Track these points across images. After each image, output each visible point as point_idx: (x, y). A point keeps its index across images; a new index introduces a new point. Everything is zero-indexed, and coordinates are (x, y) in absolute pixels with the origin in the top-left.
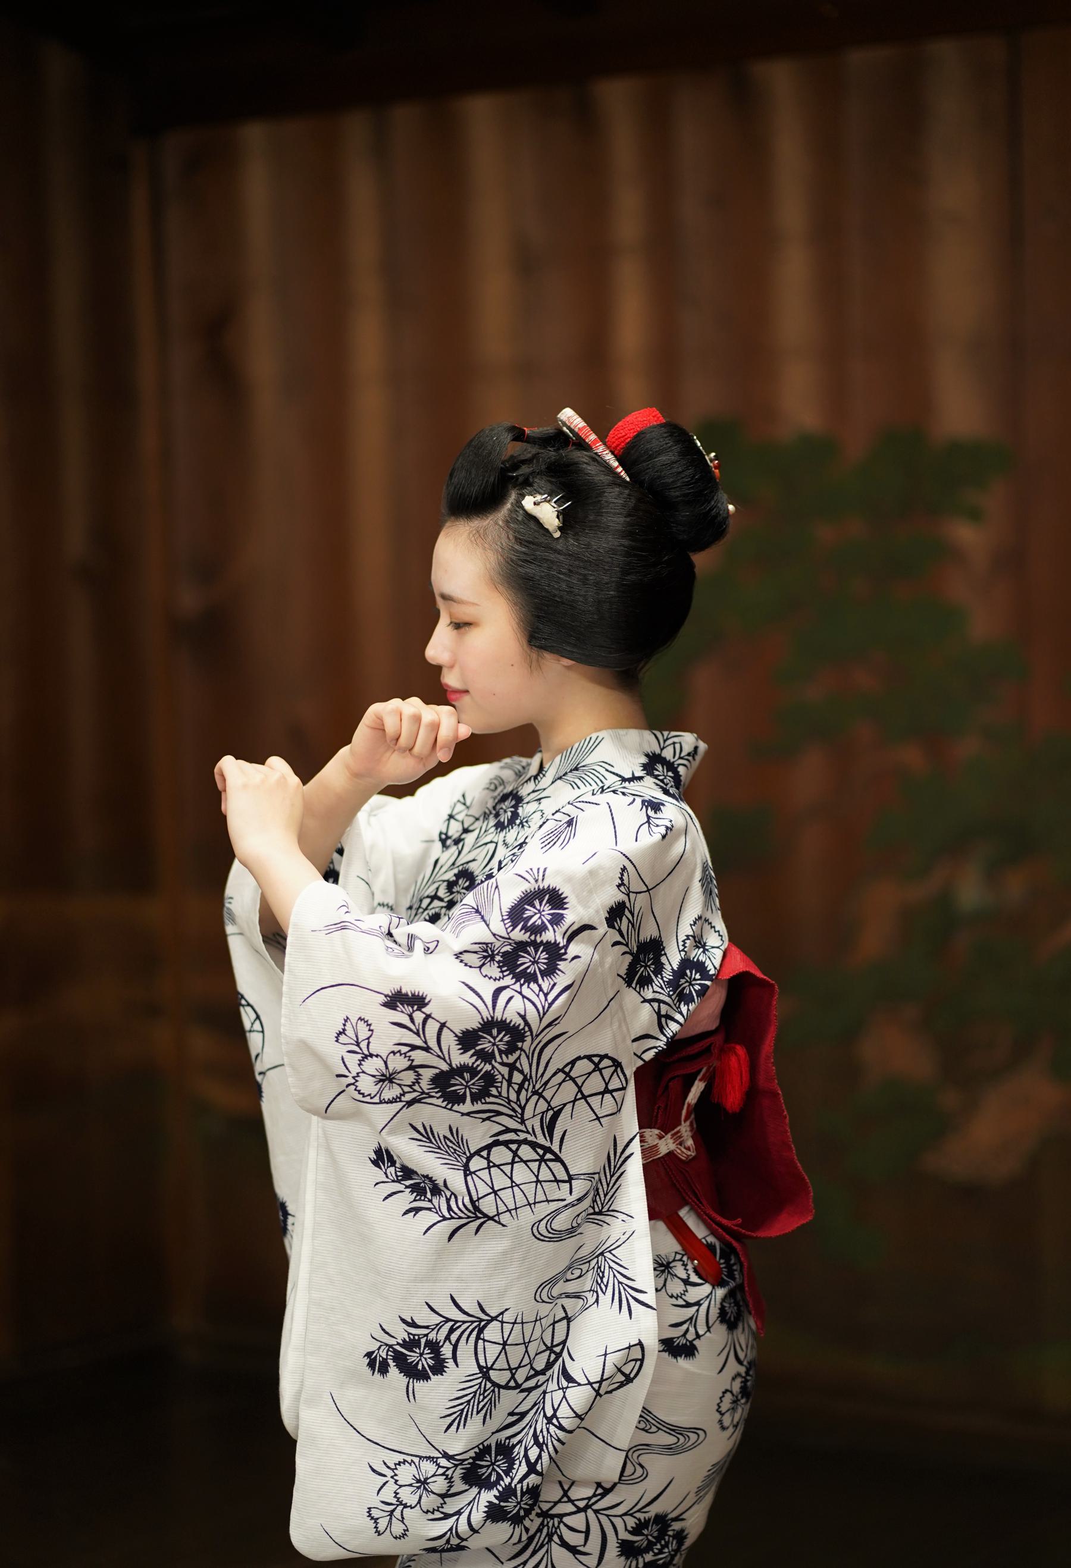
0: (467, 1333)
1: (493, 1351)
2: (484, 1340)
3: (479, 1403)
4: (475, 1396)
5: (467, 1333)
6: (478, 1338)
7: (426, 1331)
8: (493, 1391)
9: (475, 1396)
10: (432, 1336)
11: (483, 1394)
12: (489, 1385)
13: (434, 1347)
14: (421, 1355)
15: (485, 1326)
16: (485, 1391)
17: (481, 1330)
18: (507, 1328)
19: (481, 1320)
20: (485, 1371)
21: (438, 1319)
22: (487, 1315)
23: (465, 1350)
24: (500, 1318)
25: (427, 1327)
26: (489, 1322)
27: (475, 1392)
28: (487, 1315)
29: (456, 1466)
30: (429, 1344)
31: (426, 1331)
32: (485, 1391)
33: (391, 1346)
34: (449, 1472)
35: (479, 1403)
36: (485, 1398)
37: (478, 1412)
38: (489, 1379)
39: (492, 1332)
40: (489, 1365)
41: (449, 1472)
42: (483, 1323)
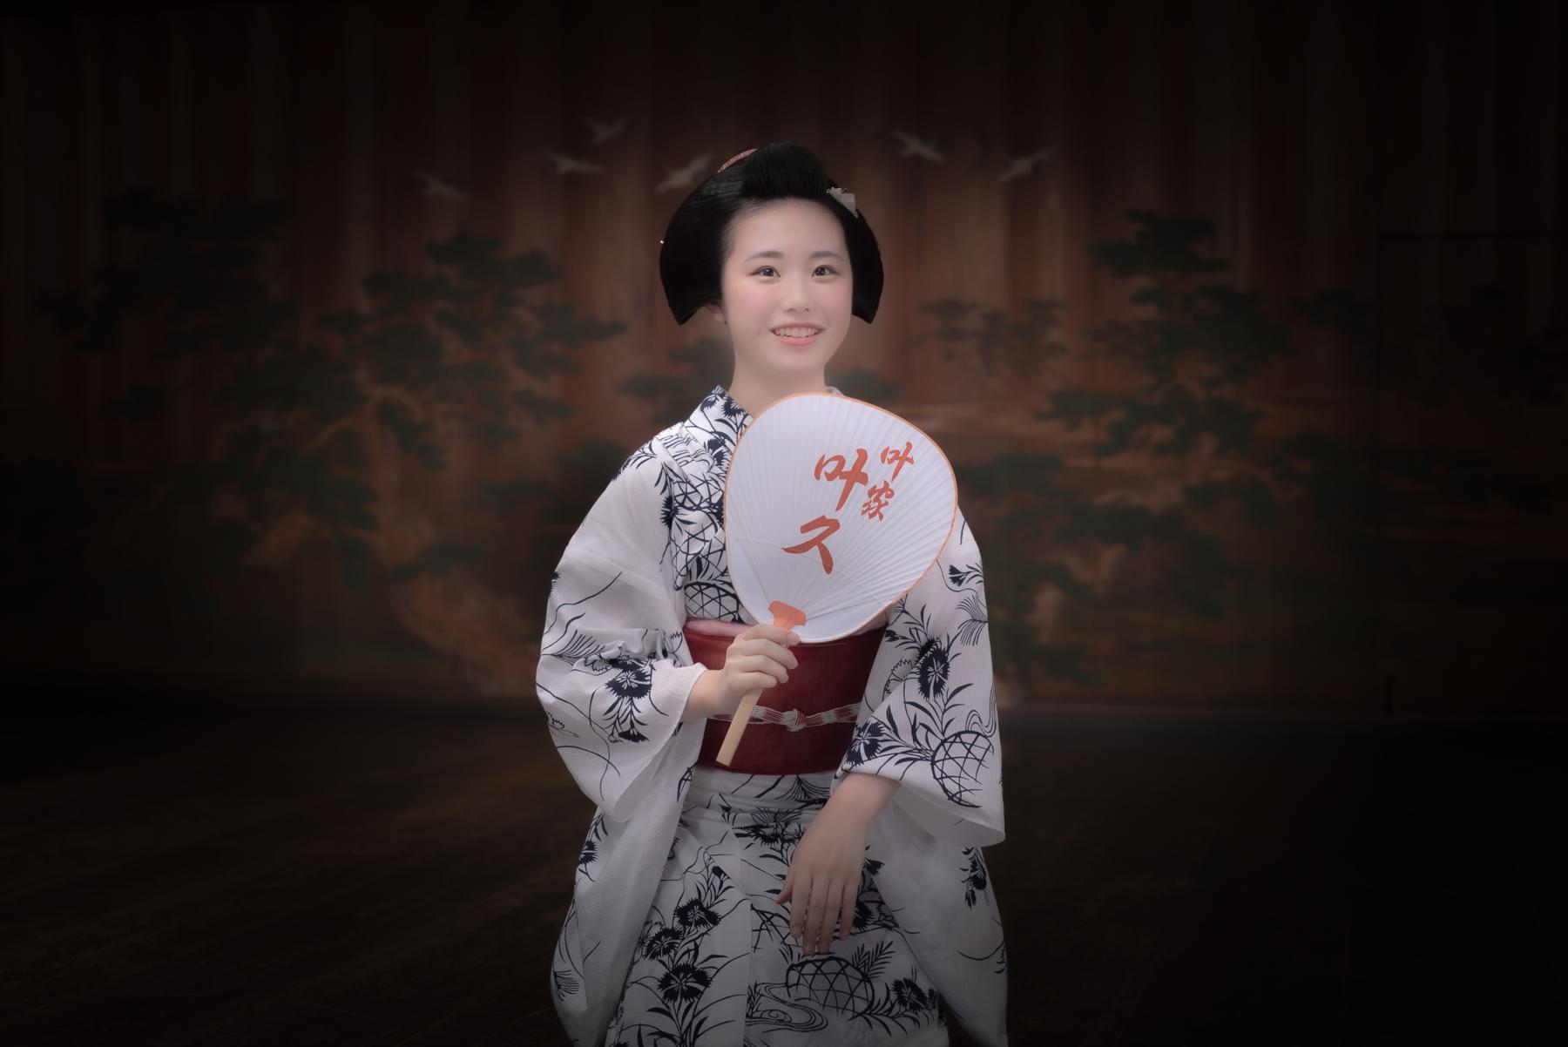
0: (880, 1007)
1: (860, 991)
2: (867, 1000)
3: (869, 959)
4: (872, 963)
5: (880, 1007)
6: (872, 1002)
7: (907, 1013)
8: (858, 965)
9: (872, 963)
10: (903, 1009)
11: (866, 964)
12: (862, 969)
13: (901, 1000)
14: (909, 997)
15: (866, 1010)
16: (864, 966)
17: (870, 1007)
18: (850, 1006)
19: (869, 1014)
20: (866, 979)
21: (899, 1020)
22: (866, 1018)
23: (881, 994)
24: (855, 1014)
25: (906, 1016)
26: (864, 1012)
27: (872, 965)
28: (866, 1018)
29: (879, 921)
30: (905, 1004)
31: (907, 1013)
32: (864, 966)
33: (927, 1008)
34: (882, 918)
35: (869, 959)
36: (865, 961)
37: (869, 953)
38: (863, 974)
39: (861, 1006)
40: (863, 983)
41: (882, 918)
42: (868, 1012)
